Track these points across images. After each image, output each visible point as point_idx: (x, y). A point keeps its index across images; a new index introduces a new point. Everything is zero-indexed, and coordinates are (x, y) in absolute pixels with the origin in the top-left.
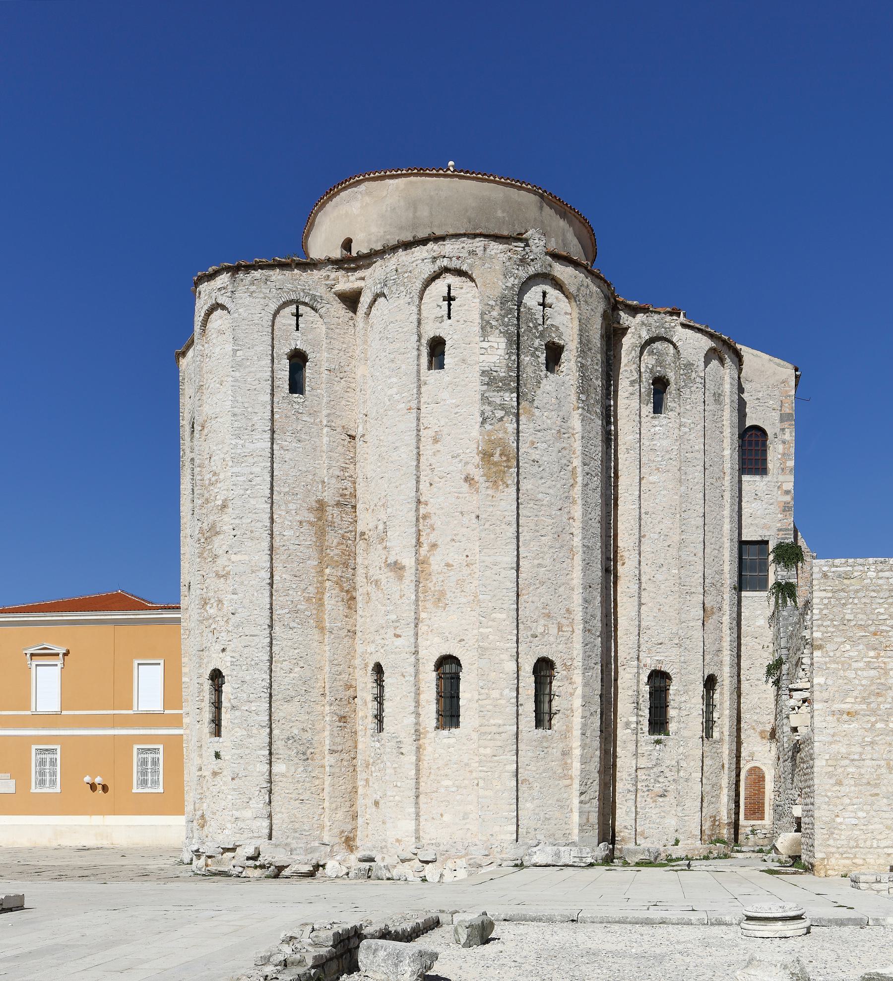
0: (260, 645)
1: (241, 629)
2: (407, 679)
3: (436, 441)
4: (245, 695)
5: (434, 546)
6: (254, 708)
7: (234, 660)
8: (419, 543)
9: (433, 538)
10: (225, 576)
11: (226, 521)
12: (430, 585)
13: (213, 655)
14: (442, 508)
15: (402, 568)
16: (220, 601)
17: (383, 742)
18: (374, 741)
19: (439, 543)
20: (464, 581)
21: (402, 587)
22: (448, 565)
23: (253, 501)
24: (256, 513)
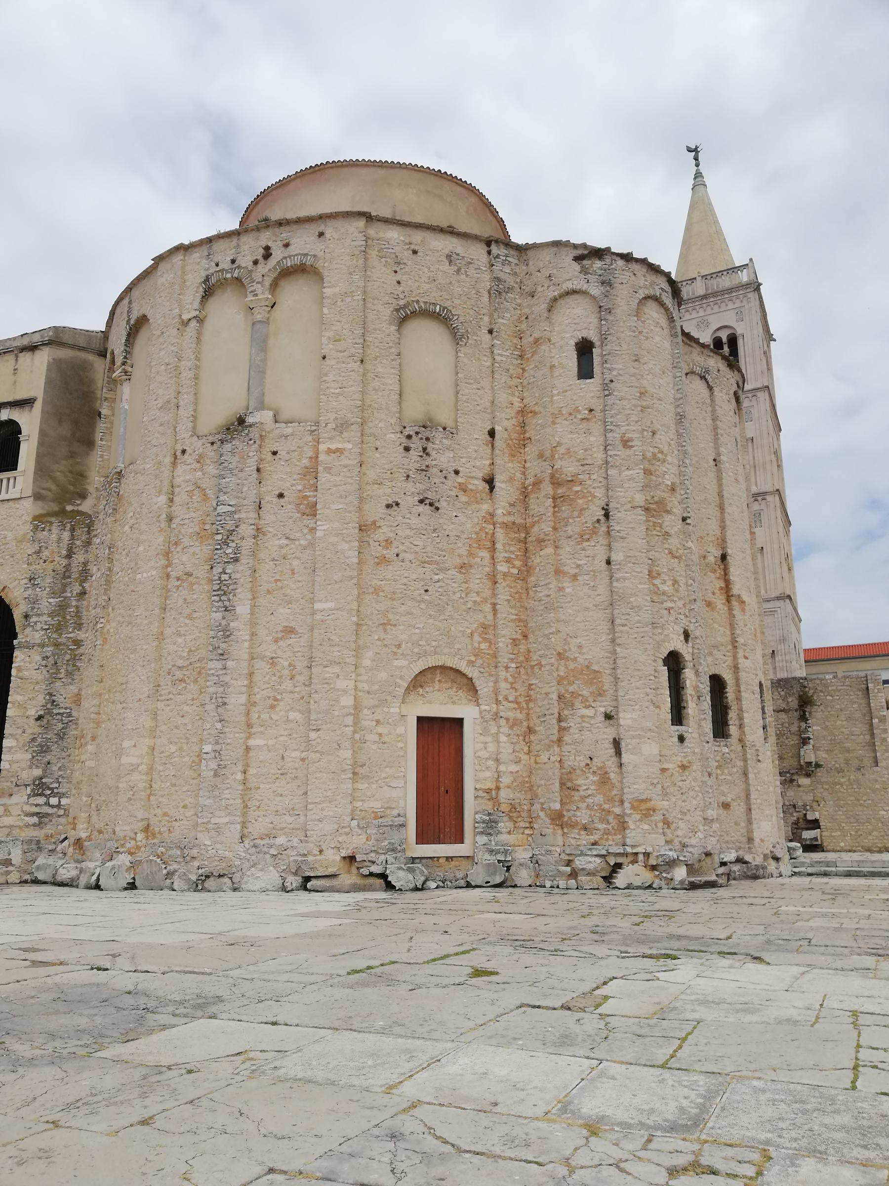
10: (679, 558)
11: (674, 503)
13: (671, 635)
15: (743, 602)
16: (675, 582)
17: (733, 748)
18: (719, 746)
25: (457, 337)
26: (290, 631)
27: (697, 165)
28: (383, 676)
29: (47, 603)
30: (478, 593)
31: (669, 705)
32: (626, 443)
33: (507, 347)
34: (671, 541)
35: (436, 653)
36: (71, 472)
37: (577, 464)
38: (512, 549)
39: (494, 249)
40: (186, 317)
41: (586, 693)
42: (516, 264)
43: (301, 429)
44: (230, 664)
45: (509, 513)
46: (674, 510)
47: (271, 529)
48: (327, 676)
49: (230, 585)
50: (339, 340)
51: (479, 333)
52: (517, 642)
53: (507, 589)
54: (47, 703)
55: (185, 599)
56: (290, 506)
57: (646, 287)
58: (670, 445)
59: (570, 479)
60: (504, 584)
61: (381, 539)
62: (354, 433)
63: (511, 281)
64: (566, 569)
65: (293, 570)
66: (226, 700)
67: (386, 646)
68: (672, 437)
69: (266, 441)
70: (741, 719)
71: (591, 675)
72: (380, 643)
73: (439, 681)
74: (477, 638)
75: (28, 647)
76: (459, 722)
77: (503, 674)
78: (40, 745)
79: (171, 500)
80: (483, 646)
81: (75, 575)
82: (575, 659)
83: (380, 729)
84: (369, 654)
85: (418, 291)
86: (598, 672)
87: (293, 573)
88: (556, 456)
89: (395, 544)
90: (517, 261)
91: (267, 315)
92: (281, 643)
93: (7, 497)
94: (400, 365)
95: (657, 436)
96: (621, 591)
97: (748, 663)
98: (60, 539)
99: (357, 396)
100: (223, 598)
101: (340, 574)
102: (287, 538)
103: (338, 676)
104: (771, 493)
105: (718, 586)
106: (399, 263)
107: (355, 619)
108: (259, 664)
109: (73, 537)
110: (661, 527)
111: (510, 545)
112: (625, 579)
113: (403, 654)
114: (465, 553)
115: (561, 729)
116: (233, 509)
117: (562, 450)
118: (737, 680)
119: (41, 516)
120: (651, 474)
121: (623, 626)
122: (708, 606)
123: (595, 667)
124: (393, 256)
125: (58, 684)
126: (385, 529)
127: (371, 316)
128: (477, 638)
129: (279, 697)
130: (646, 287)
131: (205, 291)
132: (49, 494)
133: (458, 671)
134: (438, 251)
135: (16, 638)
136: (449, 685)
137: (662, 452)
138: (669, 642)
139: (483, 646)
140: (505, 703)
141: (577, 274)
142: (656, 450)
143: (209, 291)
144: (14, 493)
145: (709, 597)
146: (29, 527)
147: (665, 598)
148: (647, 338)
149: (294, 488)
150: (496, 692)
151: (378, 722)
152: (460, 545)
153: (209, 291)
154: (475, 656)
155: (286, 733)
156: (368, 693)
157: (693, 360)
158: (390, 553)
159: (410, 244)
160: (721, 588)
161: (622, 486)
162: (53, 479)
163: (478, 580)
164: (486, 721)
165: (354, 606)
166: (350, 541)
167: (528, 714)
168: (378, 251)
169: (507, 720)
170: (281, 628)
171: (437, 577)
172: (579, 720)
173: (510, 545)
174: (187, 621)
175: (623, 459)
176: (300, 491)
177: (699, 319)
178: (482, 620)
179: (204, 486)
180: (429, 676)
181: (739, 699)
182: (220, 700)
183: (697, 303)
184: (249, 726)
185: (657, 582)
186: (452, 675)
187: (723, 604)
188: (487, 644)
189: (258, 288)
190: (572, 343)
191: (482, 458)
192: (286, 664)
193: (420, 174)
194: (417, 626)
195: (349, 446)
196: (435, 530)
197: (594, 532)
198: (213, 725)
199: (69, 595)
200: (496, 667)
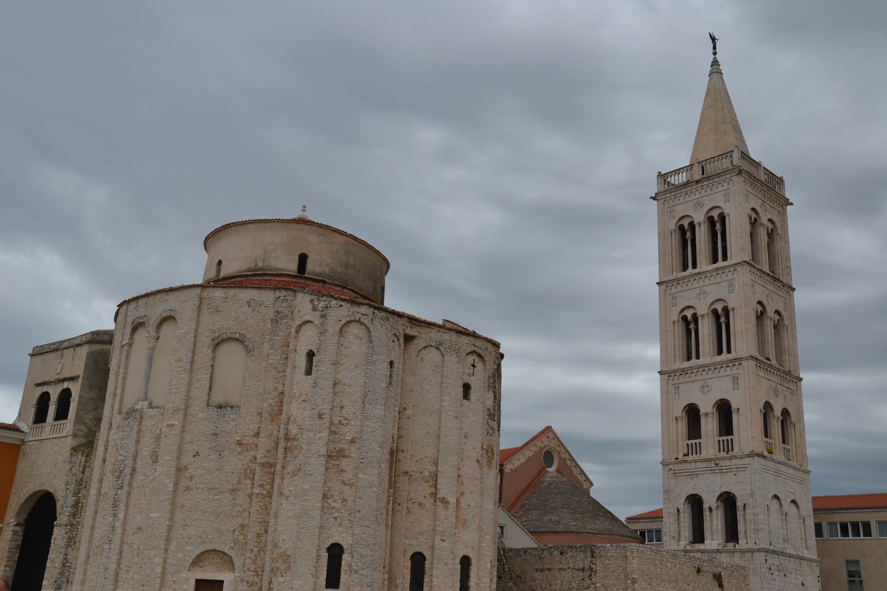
0: (371, 534)
1: (362, 522)
2: (449, 567)
3: (466, 437)
4: (361, 564)
5: (463, 493)
6: (365, 573)
7: (357, 541)
10: (351, 485)
11: (353, 451)
12: (460, 515)
13: (334, 534)
14: (467, 474)
15: (448, 502)
16: (344, 500)
20: (475, 516)
21: (448, 513)
22: (469, 506)
23: (374, 444)
24: (375, 452)
25: (248, 351)
26: (140, 528)
27: (715, 54)
28: (180, 555)
29: (71, 500)
30: (241, 506)
31: (325, 576)
32: (320, 416)
33: (278, 354)
34: (344, 474)
35: (210, 542)
36: (94, 418)
37: (298, 428)
38: (265, 478)
39: (278, 293)
40: (123, 343)
41: (282, 568)
42: (291, 300)
43: (158, 412)
44: (113, 546)
45: (266, 457)
46: (352, 455)
47: (139, 470)
48: (151, 555)
49: (118, 501)
50: (180, 361)
51: (262, 347)
52: (261, 535)
53: (258, 503)
54: (64, 560)
55: (103, 508)
56: (148, 457)
57: (348, 316)
58: (355, 413)
59: (293, 437)
60: (256, 500)
61: (188, 476)
62: (180, 415)
63: (286, 311)
64: (284, 492)
65: (145, 494)
66: (108, 566)
67: (183, 538)
68: (357, 408)
69: (144, 419)
70: (431, 581)
71: (286, 558)
72: (180, 536)
73: (213, 558)
75: (59, 526)
76: (222, 582)
78: (58, 585)
79: (106, 450)
80: (240, 538)
81: (84, 484)
82: (280, 548)
84: (174, 543)
85: (227, 327)
86: (290, 556)
87: (145, 496)
88: (290, 422)
89: (195, 479)
90: (292, 298)
91: (155, 344)
92: (136, 534)
93: (61, 435)
94: (212, 373)
95: (344, 410)
96: (305, 507)
97: (443, 544)
98: (81, 461)
99: (185, 394)
100: (115, 509)
101: (164, 497)
102: (145, 475)
103: (156, 555)
104: (746, 359)
105: (429, 492)
106: (218, 311)
107: (167, 523)
108: (125, 547)
109: (86, 461)
110: (338, 466)
111: (263, 476)
112: (308, 500)
113: (191, 543)
114: (235, 482)
116: (124, 458)
117: (292, 419)
118: (432, 555)
119: (76, 447)
120: (336, 434)
121: (303, 528)
122: (419, 506)
123: (288, 553)
124: (215, 307)
125: (70, 549)
126: (190, 470)
127: (199, 344)
128: (237, 533)
129: (131, 566)
130: (348, 316)
131: (132, 329)
132: (81, 433)
133: (224, 553)
134: (242, 300)
135: (56, 521)
136: (219, 560)
138: (332, 538)
139: (240, 538)
140: (247, 572)
141: (310, 310)
142: (342, 419)
143: (135, 329)
144: (66, 435)
145: (421, 499)
146: (68, 454)
147: (334, 511)
148: (346, 347)
149: (151, 446)
150: (244, 565)
151: (174, 582)
152: (233, 477)
153: (135, 329)
154: (234, 543)
155: (131, 586)
156: (171, 565)
157: (430, 338)
159: (226, 298)
160: (432, 494)
161: (315, 444)
162: (84, 424)
163: (241, 498)
164: (237, 583)
165: (168, 515)
166: (171, 478)
167: (262, 579)
168: (208, 305)
169: (248, 582)
170: (136, 527)
171: (216, 497)
172: (277, 584)
173: (263, 476)
174: (103, 520)
175: (318, 426)
176: (154, 448)
177: (695, 201)
178: (241, 522)
179: (117, 443)
180: (207, 555)
181: (432, 569)
182: (106, 566)
183: (694, 187)
184: (117, 581)
185: (329, 501)
186: (221, 555)
187: (431, 504)
188: (243, 537)
189: (150, 328)
190: (305, 354)
191: (254, 423)
192: (136, 547)
193: (283, 224)
194: (202, 526)
195: (177, 423)
196: (219, 469)
197: (299, 469)
198: (102, 581)
199: (80, 495)
200: (246, 550)
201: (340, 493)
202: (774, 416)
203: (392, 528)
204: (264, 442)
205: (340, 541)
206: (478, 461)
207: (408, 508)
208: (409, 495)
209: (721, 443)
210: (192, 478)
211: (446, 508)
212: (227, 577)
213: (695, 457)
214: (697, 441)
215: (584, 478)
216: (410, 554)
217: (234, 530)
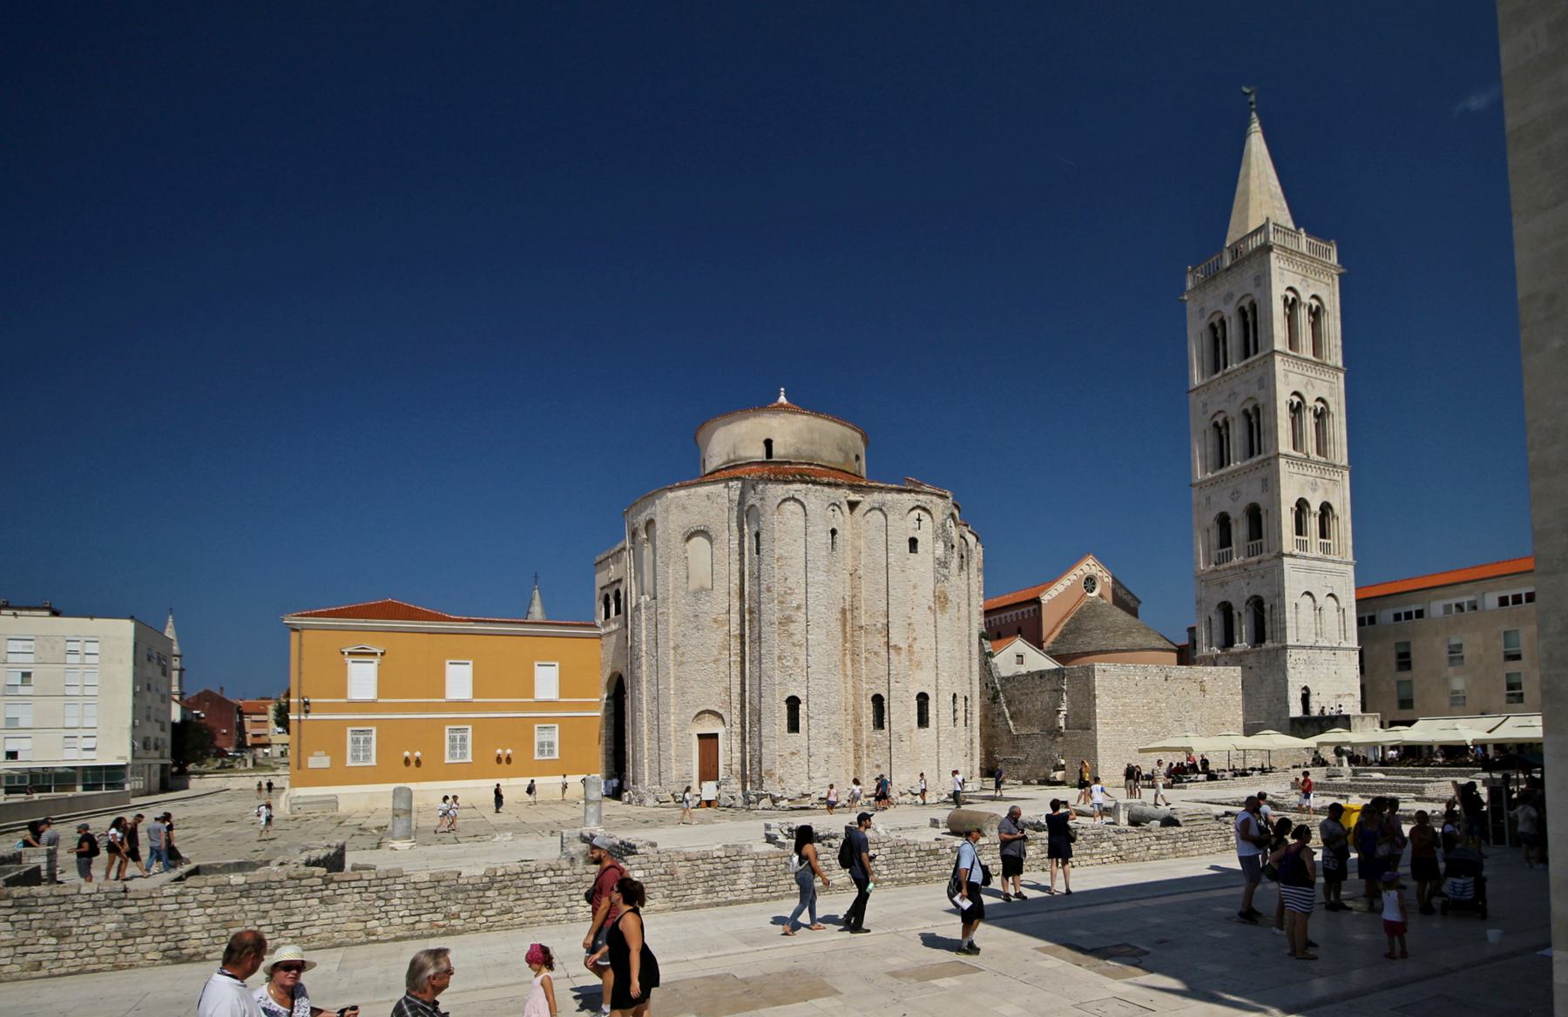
5: (915, 639)
8: (908, 638)
9: (914, 635)
10: (801, 646)
11: (800, 616)
15: (901, 649)
16: (796, 659)
19: (918, 637)
22: (922, 649)
23: (819, 607)
32: (769, 590)
34: (794, 637)
74: (723, 695)
76: (715, 736)
77: (733, 711)
83: (683, 741)
97: (898, 685)
115: (750, 737)
128: (723, 695)
137: (790, 589)
145: (876, 649)
158: (684, 659)
163: (723, 667)
169: (735, 733)
185: (784, 661)
201: (791, 654)
202: (1310, 512)
203: (856, 676)
204: (735, 618)
205: (795, 694)
206: (930, 608)
207: (866, 657)
208: (866, 646)
209: (1251, 548)
210: (683, 654)
211: (899, 654)
212: (719, 729)
213: (1226, 565)
214: (1228, 549)
215: (1130, 597)
216: (870, 696)
217: (720, 694)
